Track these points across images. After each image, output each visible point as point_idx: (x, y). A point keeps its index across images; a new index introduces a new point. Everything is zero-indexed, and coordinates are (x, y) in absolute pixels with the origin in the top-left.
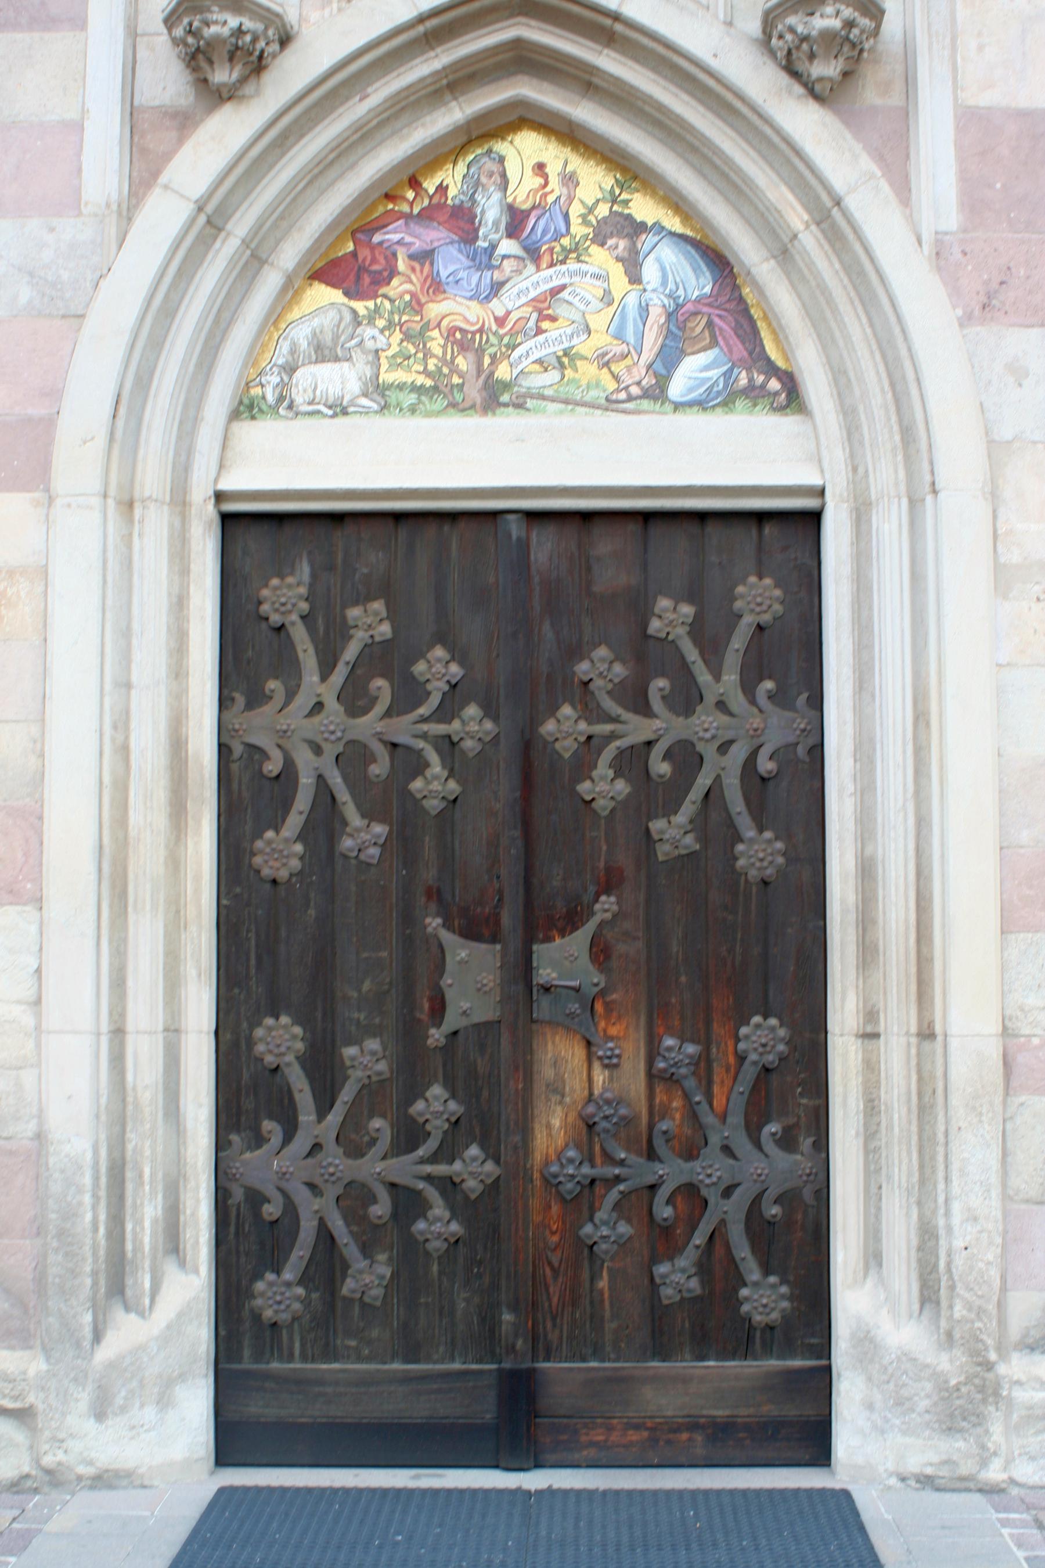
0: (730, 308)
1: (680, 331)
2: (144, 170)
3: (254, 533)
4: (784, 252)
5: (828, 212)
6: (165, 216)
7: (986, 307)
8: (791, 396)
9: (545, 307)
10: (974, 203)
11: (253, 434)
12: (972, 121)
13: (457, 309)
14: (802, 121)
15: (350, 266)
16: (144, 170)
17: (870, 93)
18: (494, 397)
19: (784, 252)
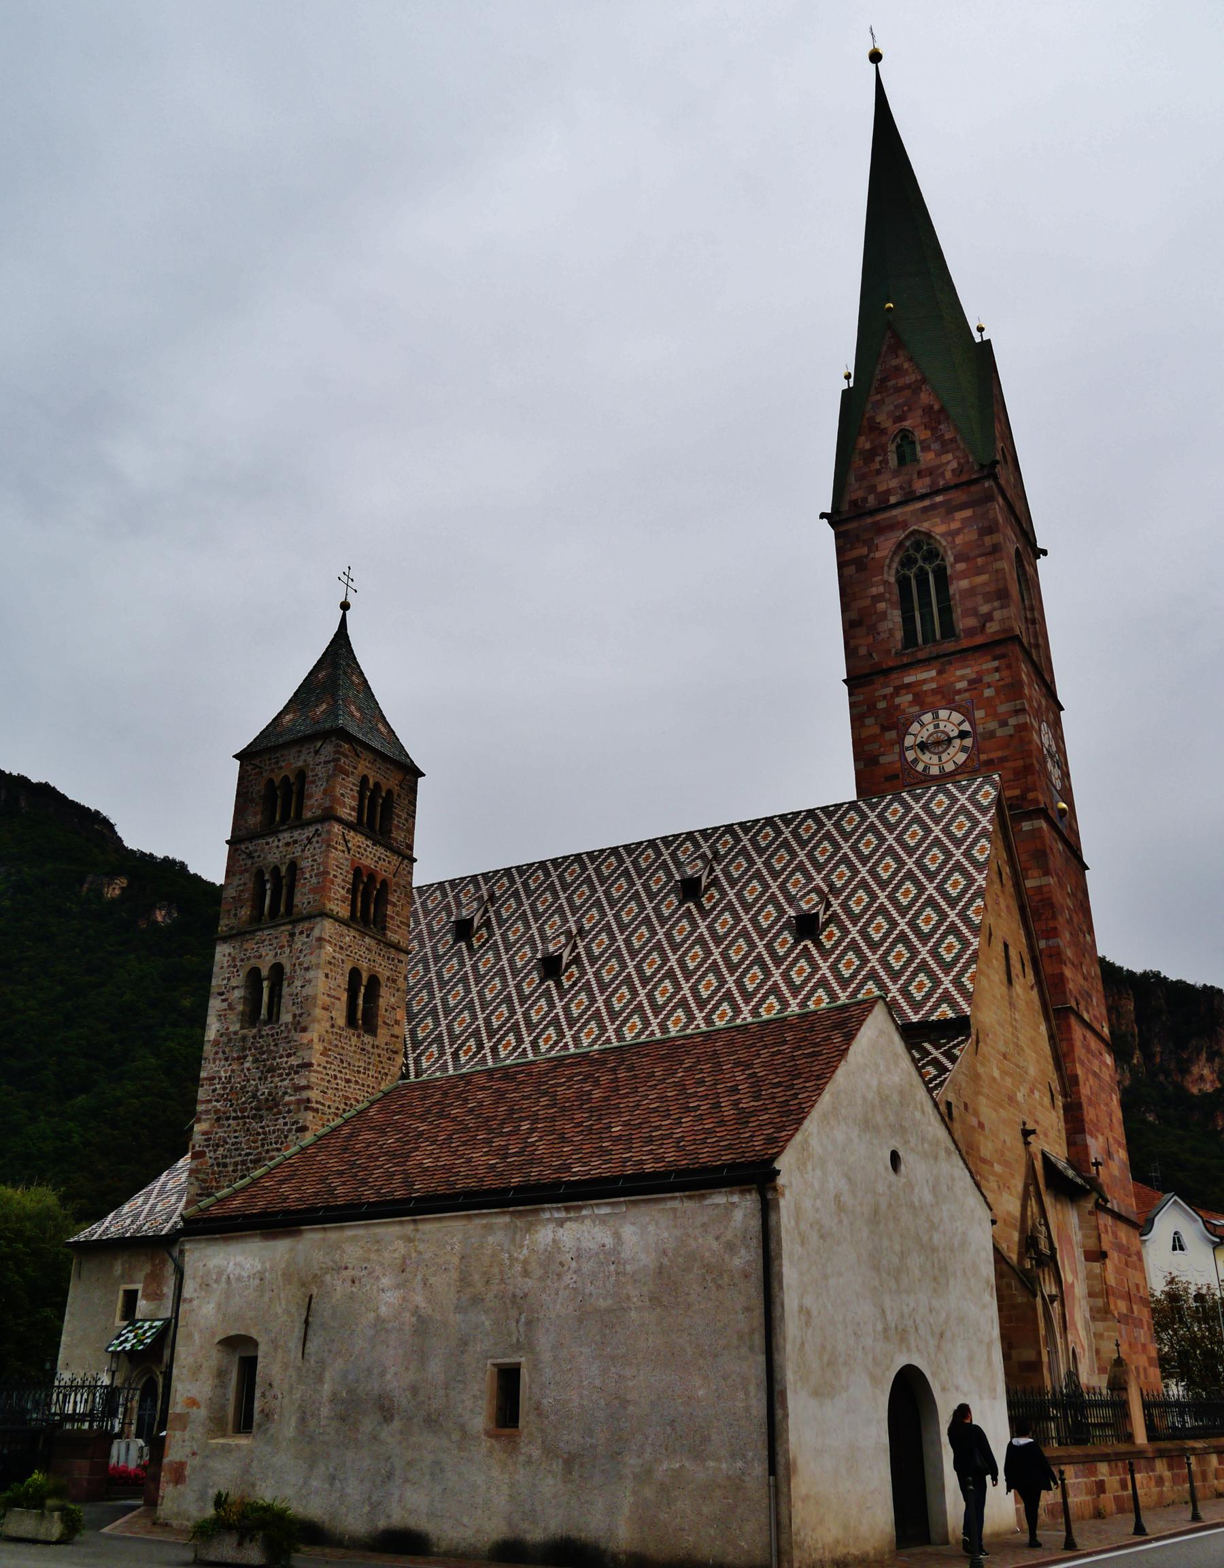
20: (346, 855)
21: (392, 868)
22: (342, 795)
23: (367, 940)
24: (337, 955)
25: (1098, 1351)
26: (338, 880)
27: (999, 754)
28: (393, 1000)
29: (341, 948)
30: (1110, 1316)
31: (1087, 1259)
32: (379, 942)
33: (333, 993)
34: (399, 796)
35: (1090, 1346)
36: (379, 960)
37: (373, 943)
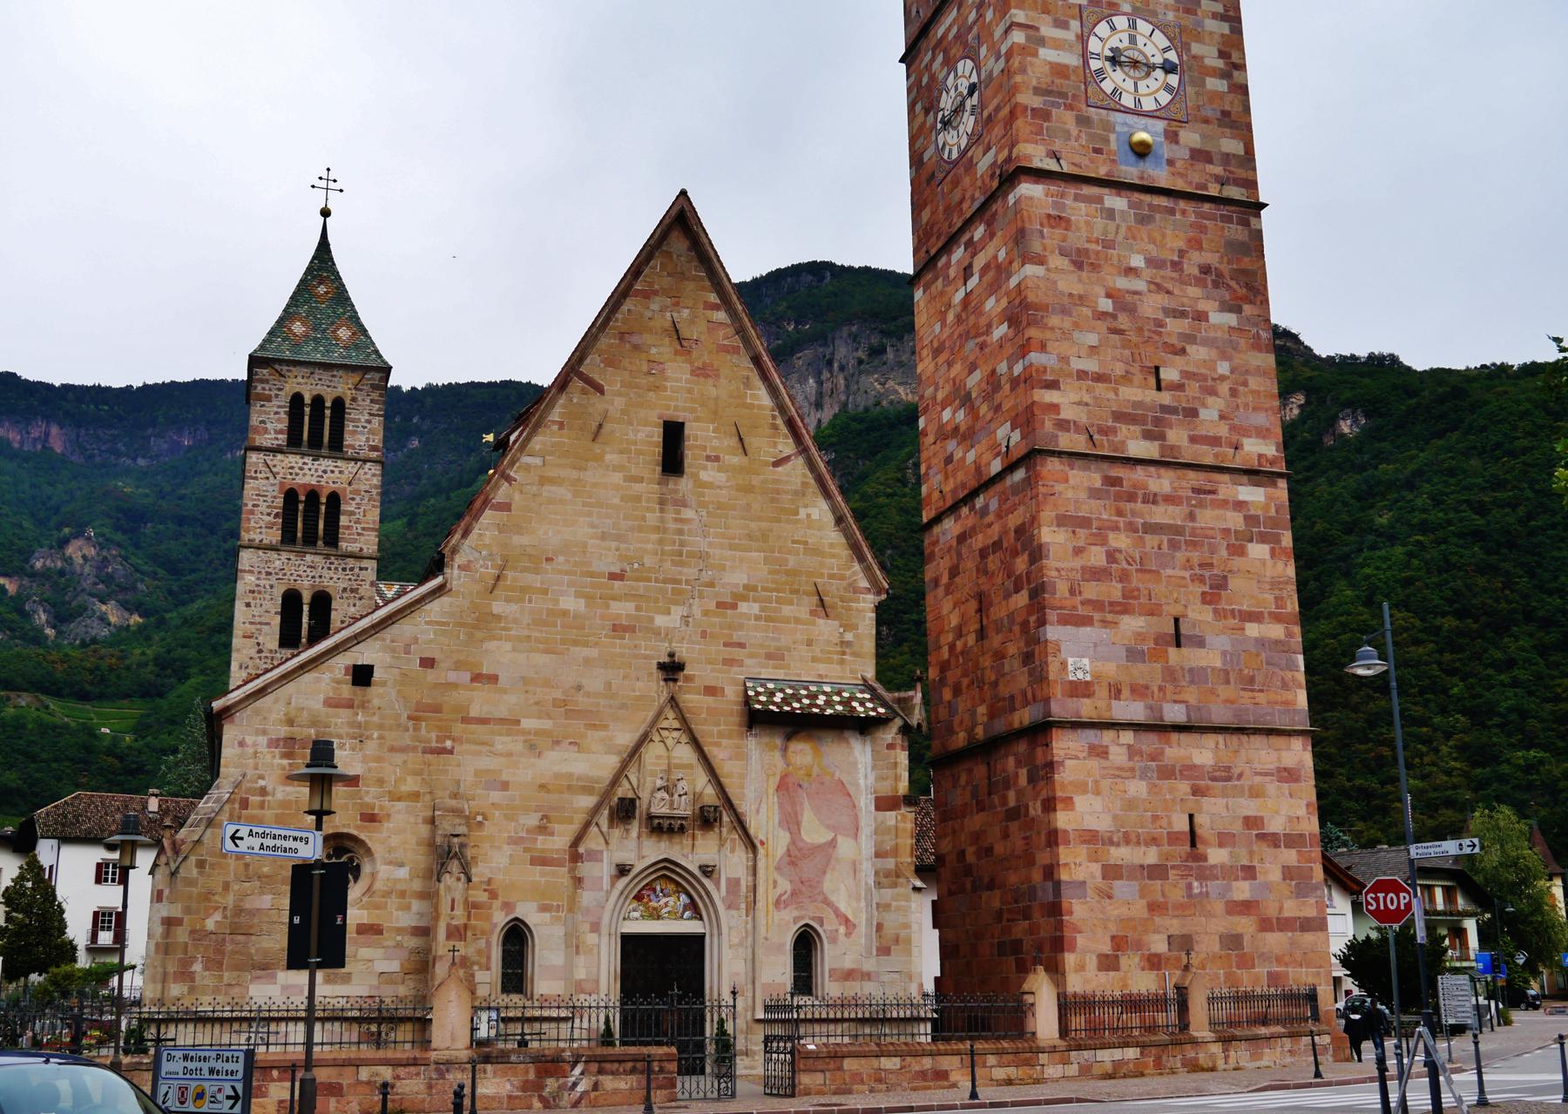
0: (693, 906)
1: (685, 908)
2: (613, 885)
3: (627, 940)
4: (701, 897)
5: (708, 893)
6: (616, 893)
7: (729, 907)
8: (701, 919)
9: (666, 905)
10: (728, 892)
11: (627, 923)
12: (728, 880)
13: (654, 904)
14: (706, 881)
15: (638, 898)
16: (613, 885)
17: (715, 876)
18: (659, 917)
19: (701, 897)
20: (272, 480)
21: (346, 477)
22: (263, 422)
23: (309, 558)
24: (262, 583)
25: (879, 927)
26: (263, 508)
27: (995, 102)
28: (353, 609)
29: (269, 574)
30: (902, 880)
31: (878, 808)
32: (327, 556)
33: (258, 620)
34: (354, 399)
35: (869, 920)
36: (325, 572)
37: (318, 559)
